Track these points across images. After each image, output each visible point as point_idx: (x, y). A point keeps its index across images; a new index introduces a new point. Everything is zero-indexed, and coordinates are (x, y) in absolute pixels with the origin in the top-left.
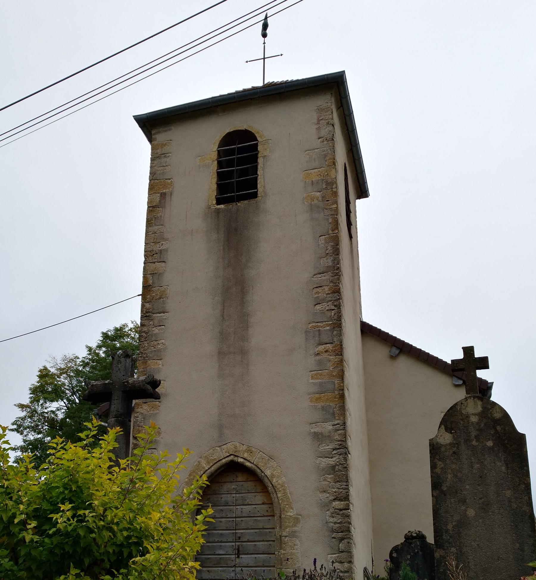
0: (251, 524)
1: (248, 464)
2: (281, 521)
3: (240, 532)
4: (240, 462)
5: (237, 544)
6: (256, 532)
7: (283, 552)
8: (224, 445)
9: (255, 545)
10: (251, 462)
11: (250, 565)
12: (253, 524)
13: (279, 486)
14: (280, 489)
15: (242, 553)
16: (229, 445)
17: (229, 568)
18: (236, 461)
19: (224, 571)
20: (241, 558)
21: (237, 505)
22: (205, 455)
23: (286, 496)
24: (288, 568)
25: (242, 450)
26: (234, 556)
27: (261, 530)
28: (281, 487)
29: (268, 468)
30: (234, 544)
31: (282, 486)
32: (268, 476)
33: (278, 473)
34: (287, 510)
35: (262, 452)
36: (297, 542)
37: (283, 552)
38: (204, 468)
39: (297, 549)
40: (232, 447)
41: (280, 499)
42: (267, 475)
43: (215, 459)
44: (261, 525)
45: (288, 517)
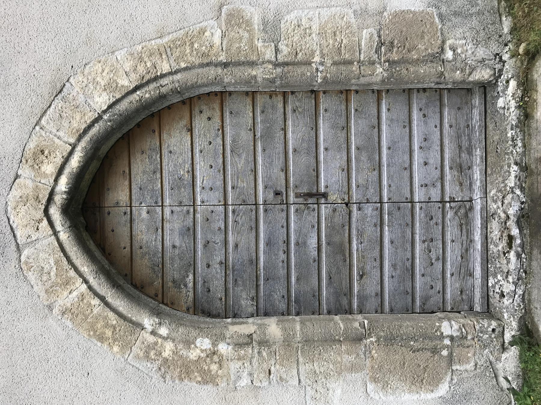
0: (243, 162)
1: (75, 162)
2: (239, 64)
3: (264, 192)
4: (68, 184)
5: (292, 199)
6: (264, 150)
7: (317, 59)
8: (15, 236)
9: (295, 150)
10: (71, 153)
11: (344, 164)
12: (244, 156)
13: (141, 69)
14: (149, 64)
15: (316, 187)
16: (16, 221)
17: (354, 219)
18: (65, 196)
19: (360, 234)
20: (327, 187)
21: (194, 202)
22: (43, 294)
23: (168, 50)
24: (360, 46)
25: (34, 181)
26: (324, 205)
27: (258, 135)
28: (143, 64)
29: (89, 100)
30: (292, 209)
31: (141, 59)
32: (112, 100)
33: (103, 71)
34: (207, 47)
35: (40, 119)
36: (291, 17)
37: (317, 59)
38: (82, 297)
39: (310, 19)
40: (23, 210)
41: (175, 67)
42: (108, 103)
43: (57, 262)
44: (246, 136)
45: (225, 43)
